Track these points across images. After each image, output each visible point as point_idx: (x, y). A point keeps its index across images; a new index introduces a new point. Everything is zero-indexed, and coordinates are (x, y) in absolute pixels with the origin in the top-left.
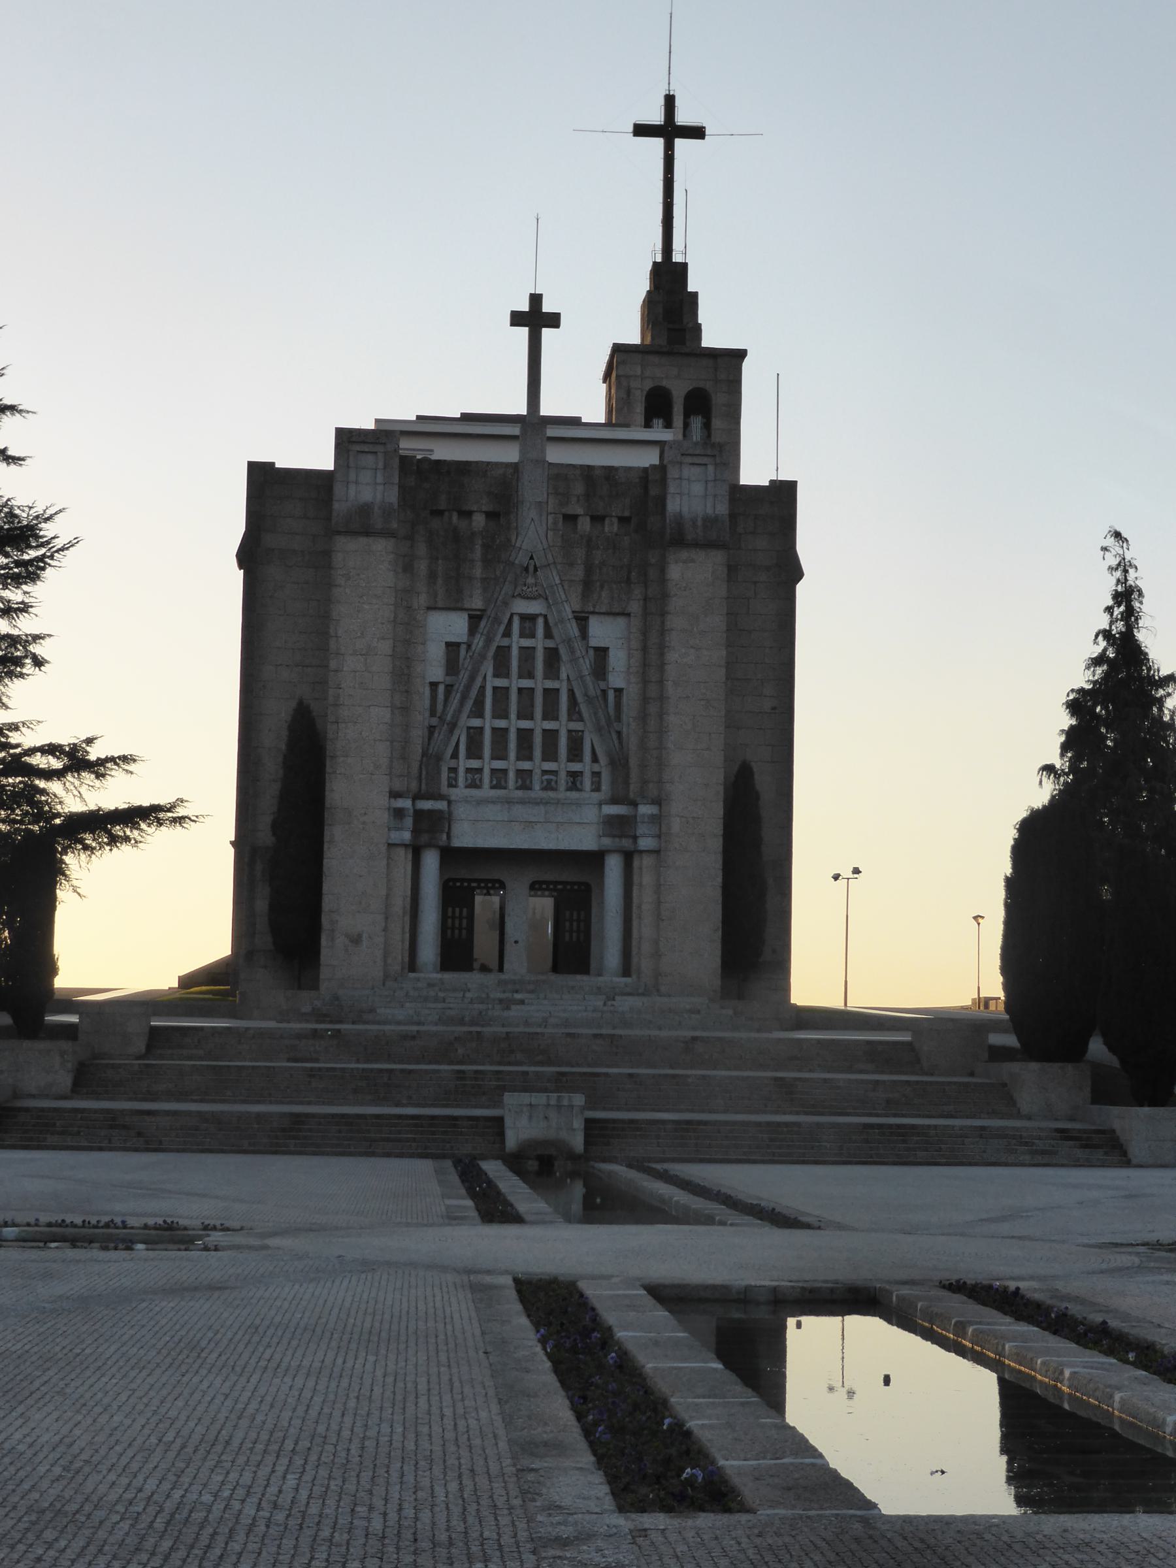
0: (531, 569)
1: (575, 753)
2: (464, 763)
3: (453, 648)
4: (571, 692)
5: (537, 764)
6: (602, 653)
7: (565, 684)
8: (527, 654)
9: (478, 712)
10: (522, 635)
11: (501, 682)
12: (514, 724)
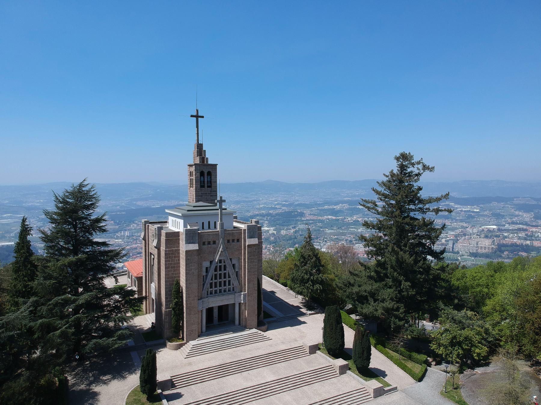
1: (229, 285)
3: (207, 268)
5: (223, 288)
6: (234, 265)
7: (228, 272)
8: (220, 266)
9: (212, 279)
11: (216, 273)
12: (218, 280)
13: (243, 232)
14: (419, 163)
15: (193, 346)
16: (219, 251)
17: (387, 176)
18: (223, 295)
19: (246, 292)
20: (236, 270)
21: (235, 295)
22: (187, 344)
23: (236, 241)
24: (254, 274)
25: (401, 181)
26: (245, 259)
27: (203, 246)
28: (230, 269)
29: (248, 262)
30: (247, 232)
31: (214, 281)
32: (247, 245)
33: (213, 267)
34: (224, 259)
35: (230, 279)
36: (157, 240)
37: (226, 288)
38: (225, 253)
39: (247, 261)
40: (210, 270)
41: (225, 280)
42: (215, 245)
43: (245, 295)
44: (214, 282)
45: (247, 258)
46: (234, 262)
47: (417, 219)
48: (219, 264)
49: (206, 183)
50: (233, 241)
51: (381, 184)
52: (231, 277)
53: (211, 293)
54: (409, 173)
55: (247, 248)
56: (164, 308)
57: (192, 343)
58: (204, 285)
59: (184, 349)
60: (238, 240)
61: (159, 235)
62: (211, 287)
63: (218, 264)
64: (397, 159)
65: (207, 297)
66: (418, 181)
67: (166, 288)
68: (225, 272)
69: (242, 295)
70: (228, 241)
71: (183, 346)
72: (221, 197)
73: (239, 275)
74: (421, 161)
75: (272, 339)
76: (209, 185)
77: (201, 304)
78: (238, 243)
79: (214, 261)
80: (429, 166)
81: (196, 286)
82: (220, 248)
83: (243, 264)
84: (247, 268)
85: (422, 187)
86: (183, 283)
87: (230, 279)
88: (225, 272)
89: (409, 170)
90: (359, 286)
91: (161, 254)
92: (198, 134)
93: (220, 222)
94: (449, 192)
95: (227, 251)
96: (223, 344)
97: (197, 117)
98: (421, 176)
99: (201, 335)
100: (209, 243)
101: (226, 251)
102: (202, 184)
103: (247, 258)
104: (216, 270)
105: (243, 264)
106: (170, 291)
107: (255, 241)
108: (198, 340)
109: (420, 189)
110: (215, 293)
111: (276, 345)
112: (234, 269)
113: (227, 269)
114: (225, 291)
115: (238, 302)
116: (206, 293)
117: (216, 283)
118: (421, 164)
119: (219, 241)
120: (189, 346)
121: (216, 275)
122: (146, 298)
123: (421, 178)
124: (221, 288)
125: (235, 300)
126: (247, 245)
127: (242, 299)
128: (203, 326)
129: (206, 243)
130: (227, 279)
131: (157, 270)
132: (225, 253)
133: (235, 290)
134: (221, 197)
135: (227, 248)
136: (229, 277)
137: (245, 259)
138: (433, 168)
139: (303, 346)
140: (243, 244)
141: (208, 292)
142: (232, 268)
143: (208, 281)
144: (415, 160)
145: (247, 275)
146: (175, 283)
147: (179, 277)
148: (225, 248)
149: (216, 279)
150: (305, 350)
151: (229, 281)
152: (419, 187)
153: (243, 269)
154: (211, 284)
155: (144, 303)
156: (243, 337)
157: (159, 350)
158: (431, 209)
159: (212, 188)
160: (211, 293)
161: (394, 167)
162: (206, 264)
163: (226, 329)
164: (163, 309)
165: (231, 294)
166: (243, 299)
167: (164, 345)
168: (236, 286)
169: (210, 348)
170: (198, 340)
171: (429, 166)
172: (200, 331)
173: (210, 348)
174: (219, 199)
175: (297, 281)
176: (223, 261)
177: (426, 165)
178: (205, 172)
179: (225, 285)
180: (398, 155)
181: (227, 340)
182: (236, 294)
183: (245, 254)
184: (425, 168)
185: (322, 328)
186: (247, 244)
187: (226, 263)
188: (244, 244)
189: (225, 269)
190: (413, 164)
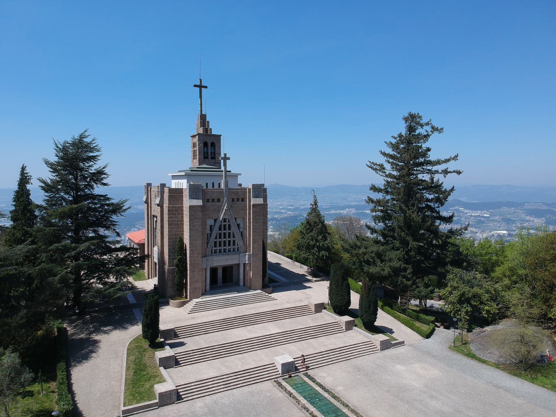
0: (227, 210)
1: (234, 244)
2: (214, 249)
3: (211, 226)
4: (233, 232)
5: (227, 247)
6: (238, 225)
7: (232, 231)
8: (225, 225)
10: (224, 222)
11: (220, 232)
12: (223, 240)
13: (248, 192)
14: (427, 124)
15: (196, 302)
16: (223, 209)
17: (395, 138)
18: (228, 254)
19: (251, 253)
20: (241, 231)
21: (239, 255)
22: (190, 302)
23: (240, 200)
24: (259, 235)
25: (409, 143)
26: (249, 219)
27: (207, 203)
28: (234, 229)
29: (253, 222)
30: (252, 191)
31: (218, 240)
32: (252, 205)
33: (217, 225)
34: (228, 219)
35: (234, 239)
36: (159, 198)
37: (230, 248)
38: (230, 212)
39: (252, 221)
40: (214, 228)
41: (229, 239)
42: (219, 203)
43: (249, 256)
44: (218, 241)
45: (252, 218)
46: (239, 221)
47: (425, 181)
48: (223, 223)
49: (210, 154)
50: (238, 200)
51: (389, 144)
52: (236, 236)
53: (215, 252)
54: (418, 135)
55: (252, 207)
56: (166, 267)
57: (195, 300)
58: (208, 243)
59: (188, 306)
60: (243, 200)
61: (162, 193)
62: (215, 246)
63: (223, 223)
64: (406, 119)
65: (211, 256)
66: (427, 142)
67: (169, 246)
68: (230, 231)
69: (247, 256)
70: (233, 200)
71: (186, 304)
72: (225, 154)
73: (243, 235)
74: (430, 123)
75: (277, 299)
76: (213, 156)
77: (206, 261)
78: (243, 203)
79: (218, 219)
80: (438, 127)
81: (200, 243)
82: (224, 206)
83: (248, 224)
84: (252, 228)
85: (431, 148)
86: (187, 241)
87: (234, 239)
88: (230, 231)
89: (417, 132)
90: (366, 248)
91: (164, 212)
92: (201, 104)
93: (224, 180)
94: (458, 154)
95: (231, 210)
96: (227, 302)
97: (201, 87)
98: (429, 137)
99: (205, 293)
100: (213, 200)
101: (231, 210)
102: (206, 155)
103: (252, 218)
104: (220, 229)
105: (248, 224)
106: (174, 248)
107: (260, 201)
108: (201, 298)
109: (429, 150)
110: (219, 252)
111: (281, 304)
112: (239, 229)
113: (232, 228)
114: (229, 251)
115: (243, 262)
116: (211, 252)
117: (220, 242)
118: (430, 125)
119: (224, 200)
120: (193, 303)
121: (220, 234)
122: (148, 256)
123: (430, 139)
124: (225, 248)
125: (240, 261)
126: (252, 205)
127: (247, 259)
128: (207, 285)
129: (210, 200)
130: (232, 239)
131: (160, 228)
132: (230, 212)
133: (240, 251)
134: (225, 154)
135: (231, 207)
136: (234, 237)
137: (249, 219)
138: (442, 129)
139: (308, 305)
140: (248, 203)
141: (212, 250)
142: (237, 227)
143: (212, 239)
144: (423, 121)
145: (251, 235)
146: (178, 239)
147: (183, 234)
148: (230, 207)
149: (220, 238)
150: (311, 308)
151: (234, 241)
152: (428, 148)
153: (248, 230)
154: (215, 243)
155: (147, 261)
156: (248, 297)
157: (162, 308)
158: (440, 171)
159: (216, 160)
160: (215, 252)
161: (402, 129)
162: (210, 222)
163: (230, 289)
164: (166, 267)
165: (235, 253)
166: (248, 259)
167: (167, 304)
168: (241, 247)
169: (214, 306)
170: (201, 298)
171: (437, 128)
172: (204, 290)
173: (214, 306)
174: (222, 155)
175: (303, 247)
176: (228, 220)
177: (434, 126)
178: (209, 142)
179: (229, 245)
180: (407, 115)
181: (231, 299)
182: (240, 254)
183: (249, 213)
184: (434, 129)
185: (328, 287)
186: (252, 203)
187: (231, 223)
188: (248, 203)
189: (229, 229)
190: (422, 126)
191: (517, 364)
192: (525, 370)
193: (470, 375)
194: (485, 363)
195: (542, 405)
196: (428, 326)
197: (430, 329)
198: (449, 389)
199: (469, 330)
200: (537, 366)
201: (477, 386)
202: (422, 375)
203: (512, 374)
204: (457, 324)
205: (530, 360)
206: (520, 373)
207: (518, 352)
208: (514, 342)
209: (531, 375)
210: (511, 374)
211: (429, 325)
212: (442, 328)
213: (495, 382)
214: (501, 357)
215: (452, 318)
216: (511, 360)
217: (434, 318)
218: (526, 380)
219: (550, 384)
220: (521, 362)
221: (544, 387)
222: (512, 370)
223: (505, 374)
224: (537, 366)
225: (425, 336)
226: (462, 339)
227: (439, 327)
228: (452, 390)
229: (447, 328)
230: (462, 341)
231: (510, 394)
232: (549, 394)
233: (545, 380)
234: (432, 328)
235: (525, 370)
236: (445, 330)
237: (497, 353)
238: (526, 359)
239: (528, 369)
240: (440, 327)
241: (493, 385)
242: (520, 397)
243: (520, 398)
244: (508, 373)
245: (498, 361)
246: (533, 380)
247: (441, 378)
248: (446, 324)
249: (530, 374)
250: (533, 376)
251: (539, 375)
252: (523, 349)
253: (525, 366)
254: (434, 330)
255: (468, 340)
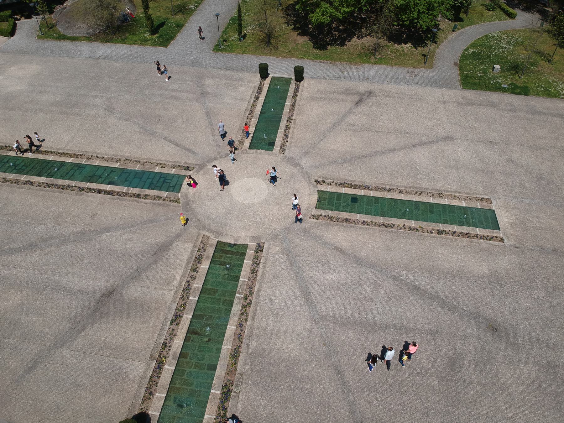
191: (105, 30)
192: (115, 34)
193: (68, 57)
194: (78, 40)
195: (139, 61)
196: (7, 23)
197: (11, 25)
198: (54, 78)
199: (51, 12)
200: (123, 26)
201: (78, 64)
202: (23, 76)
203: (105, 41)
204: (36, 9)
205: (114, 22)
206: (111, 39)
207: (102, 18)
208: (95, 9)
209: (121, 37)
210: (103, 42)
211: (8, 21)
212: (23, 20)
213: (93, 55)
214: (89, 28)
215: (28, 4)
216: (99, 29)
217: (10, 11)
218: (118, 43)
219: (139, 40)
220: (108, 27)
221: (135, 44)
222: (103, 38)
223: (98, 43)
224: (123, 26)
225: (8, 35)
226: (47, 23)
227: (19, 20)
228: (57, 78)
229: (28, 17)
230: (47, 25)
231: (109, 61)
232: (141, 49)
233: (135, 38)
234: (12, 23)
235: (115, 34)
236: (26, 20)
237: (83, 26)
238: (111, 23)
239: (116, 32)
240: (21, 19)
241: (92, 59)
242: (119, 60)
243: (119, 61)
244: (101, 42)
245: (88, 34)
246: (124, 41)
247: (42, 72)
248: (26, 14)
249: (120, 36)
250: (123, 37)
251: (128, 34)
252: (105, 14)
253: (113, 30)
254: (15, 25)
255: (54, 22)
